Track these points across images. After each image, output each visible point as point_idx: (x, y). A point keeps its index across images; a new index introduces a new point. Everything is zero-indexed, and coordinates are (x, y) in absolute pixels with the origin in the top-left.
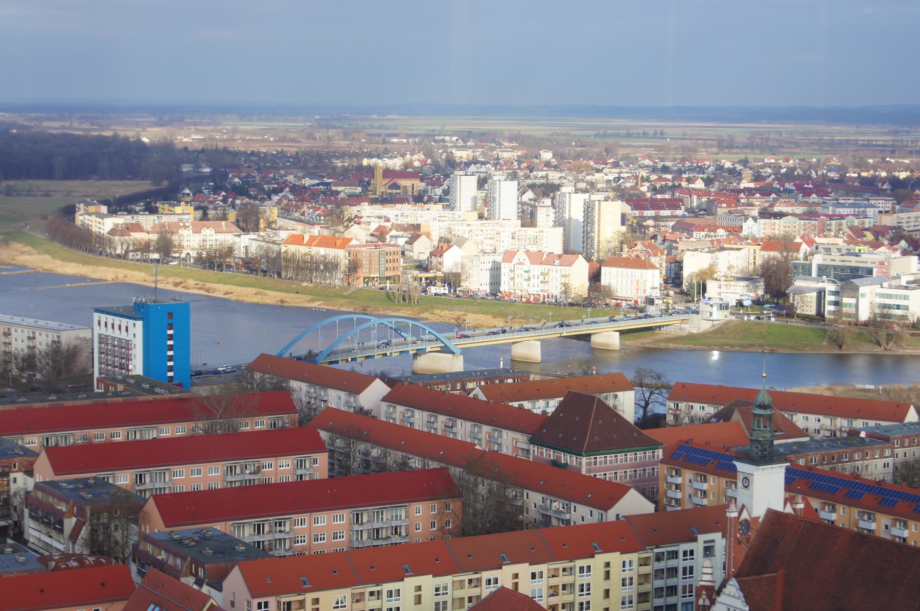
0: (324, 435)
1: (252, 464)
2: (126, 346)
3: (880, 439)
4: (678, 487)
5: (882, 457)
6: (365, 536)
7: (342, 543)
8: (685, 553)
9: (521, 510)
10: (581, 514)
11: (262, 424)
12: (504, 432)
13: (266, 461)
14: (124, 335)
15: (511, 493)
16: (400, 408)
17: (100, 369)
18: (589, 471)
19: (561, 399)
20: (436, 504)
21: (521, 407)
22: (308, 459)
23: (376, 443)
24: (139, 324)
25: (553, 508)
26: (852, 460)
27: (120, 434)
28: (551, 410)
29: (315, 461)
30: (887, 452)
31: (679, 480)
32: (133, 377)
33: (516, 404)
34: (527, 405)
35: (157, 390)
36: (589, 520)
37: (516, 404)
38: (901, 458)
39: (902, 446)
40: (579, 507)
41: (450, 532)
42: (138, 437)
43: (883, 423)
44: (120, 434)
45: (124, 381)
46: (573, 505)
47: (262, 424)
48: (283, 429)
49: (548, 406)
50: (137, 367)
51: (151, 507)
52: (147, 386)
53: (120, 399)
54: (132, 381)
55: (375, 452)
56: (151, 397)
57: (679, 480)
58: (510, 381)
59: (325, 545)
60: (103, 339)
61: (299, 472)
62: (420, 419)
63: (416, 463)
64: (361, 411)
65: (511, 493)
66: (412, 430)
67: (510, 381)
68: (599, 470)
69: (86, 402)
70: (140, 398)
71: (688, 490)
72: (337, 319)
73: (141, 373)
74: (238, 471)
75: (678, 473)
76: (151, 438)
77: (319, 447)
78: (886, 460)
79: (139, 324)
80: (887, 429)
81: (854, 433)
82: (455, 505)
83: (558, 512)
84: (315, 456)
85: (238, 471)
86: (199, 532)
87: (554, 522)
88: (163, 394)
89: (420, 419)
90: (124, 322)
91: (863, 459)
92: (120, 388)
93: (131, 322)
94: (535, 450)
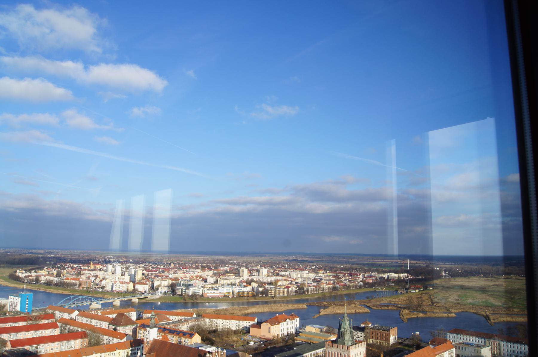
0: (58, 323)
1: (39, 332)
2: (16, 304)
3: (186, 321)
4: (141, 333)
5: (186, 325)
6: (64, 348)
7: (58, 350)
8: (138, 349)
9: (103, 341)
10: (117, 341)
11: (46, 321)
12: (104, 322)
13: (43, 331)
14: (16, 301)
15: (101, 337)
16: (80, 317)
17: (9, 309)
18: (122, 331)
19: (116, 315)
20: (82, 340)
21: (108, 316)
22: (54, 330)
23: (71, 325)
24: (20, 298)
25: (110, 340)
26: (180, 326)
27: (8, 325)
28: (114, 317)
29: (56, 330)
30: (188, 324)
31: (141, 332)
32: (16, 311)
33: (106, 316)
34: (109, 316)
35: (21, 314)
36: (118, 342)
37: (106, 316)
38: (191, 325)
39: (191, 322)
40: (116, 339)
41: (85, 347)
42: (13, 326)
43: (186, 317)
44: (8, 325)
45: (14, 312)
46: (115, 339)
47: (46, 321)
48: (51, 323)
49: (114, 316)
50: (18, 309)
51: (9, 344)
52: (19, 313)
53: (11, 317)
54: (16, 312)
55: (71, 328)
56: (19, 316)
57: (141, 332)
58: (108, 310)
59: (54, 351)
60: (11, 302)
61: (51, 333)
62: (85, 320)
63: (80, 330)
64: (72, 319)
65: (101, 337)
66: (83, 323)
67: (108, 310)
68: (124, 330)
69: (2, 317)
70: (16, 316)
71: (143, 334)
72: (71, 297)
73: (19, 310)
74: (36, 333)
75: (141, 331)
76: (17, 326)
77: (57, 327)
78: (187, 326)
79: (20, 298)
80: (188, 318)
81: (181, 320)
82: (86, 340)
83: (111, 341)
84: (56, 329)
85: (36, 333)
86: (19, 349)
87: (111, 343)
88: (22, 315)
89: (85, 320)
90: (16, 298)
91: (182, 325)
92: (12, 314)
93: (18, 298)
94: (110, 326)
